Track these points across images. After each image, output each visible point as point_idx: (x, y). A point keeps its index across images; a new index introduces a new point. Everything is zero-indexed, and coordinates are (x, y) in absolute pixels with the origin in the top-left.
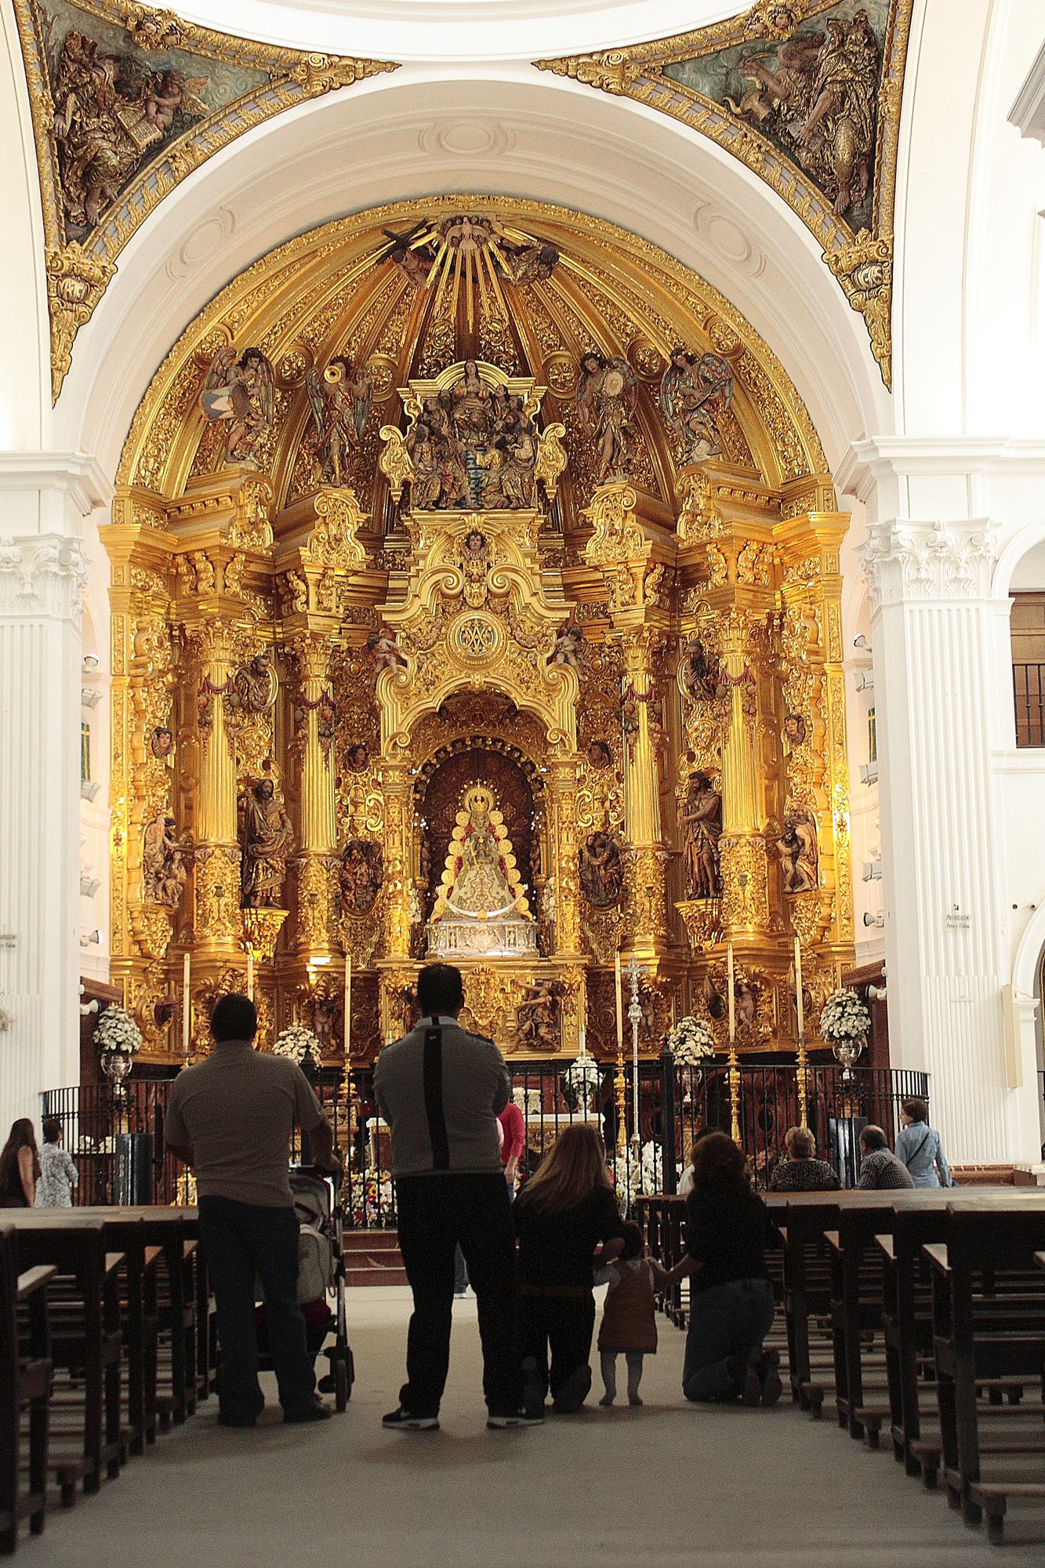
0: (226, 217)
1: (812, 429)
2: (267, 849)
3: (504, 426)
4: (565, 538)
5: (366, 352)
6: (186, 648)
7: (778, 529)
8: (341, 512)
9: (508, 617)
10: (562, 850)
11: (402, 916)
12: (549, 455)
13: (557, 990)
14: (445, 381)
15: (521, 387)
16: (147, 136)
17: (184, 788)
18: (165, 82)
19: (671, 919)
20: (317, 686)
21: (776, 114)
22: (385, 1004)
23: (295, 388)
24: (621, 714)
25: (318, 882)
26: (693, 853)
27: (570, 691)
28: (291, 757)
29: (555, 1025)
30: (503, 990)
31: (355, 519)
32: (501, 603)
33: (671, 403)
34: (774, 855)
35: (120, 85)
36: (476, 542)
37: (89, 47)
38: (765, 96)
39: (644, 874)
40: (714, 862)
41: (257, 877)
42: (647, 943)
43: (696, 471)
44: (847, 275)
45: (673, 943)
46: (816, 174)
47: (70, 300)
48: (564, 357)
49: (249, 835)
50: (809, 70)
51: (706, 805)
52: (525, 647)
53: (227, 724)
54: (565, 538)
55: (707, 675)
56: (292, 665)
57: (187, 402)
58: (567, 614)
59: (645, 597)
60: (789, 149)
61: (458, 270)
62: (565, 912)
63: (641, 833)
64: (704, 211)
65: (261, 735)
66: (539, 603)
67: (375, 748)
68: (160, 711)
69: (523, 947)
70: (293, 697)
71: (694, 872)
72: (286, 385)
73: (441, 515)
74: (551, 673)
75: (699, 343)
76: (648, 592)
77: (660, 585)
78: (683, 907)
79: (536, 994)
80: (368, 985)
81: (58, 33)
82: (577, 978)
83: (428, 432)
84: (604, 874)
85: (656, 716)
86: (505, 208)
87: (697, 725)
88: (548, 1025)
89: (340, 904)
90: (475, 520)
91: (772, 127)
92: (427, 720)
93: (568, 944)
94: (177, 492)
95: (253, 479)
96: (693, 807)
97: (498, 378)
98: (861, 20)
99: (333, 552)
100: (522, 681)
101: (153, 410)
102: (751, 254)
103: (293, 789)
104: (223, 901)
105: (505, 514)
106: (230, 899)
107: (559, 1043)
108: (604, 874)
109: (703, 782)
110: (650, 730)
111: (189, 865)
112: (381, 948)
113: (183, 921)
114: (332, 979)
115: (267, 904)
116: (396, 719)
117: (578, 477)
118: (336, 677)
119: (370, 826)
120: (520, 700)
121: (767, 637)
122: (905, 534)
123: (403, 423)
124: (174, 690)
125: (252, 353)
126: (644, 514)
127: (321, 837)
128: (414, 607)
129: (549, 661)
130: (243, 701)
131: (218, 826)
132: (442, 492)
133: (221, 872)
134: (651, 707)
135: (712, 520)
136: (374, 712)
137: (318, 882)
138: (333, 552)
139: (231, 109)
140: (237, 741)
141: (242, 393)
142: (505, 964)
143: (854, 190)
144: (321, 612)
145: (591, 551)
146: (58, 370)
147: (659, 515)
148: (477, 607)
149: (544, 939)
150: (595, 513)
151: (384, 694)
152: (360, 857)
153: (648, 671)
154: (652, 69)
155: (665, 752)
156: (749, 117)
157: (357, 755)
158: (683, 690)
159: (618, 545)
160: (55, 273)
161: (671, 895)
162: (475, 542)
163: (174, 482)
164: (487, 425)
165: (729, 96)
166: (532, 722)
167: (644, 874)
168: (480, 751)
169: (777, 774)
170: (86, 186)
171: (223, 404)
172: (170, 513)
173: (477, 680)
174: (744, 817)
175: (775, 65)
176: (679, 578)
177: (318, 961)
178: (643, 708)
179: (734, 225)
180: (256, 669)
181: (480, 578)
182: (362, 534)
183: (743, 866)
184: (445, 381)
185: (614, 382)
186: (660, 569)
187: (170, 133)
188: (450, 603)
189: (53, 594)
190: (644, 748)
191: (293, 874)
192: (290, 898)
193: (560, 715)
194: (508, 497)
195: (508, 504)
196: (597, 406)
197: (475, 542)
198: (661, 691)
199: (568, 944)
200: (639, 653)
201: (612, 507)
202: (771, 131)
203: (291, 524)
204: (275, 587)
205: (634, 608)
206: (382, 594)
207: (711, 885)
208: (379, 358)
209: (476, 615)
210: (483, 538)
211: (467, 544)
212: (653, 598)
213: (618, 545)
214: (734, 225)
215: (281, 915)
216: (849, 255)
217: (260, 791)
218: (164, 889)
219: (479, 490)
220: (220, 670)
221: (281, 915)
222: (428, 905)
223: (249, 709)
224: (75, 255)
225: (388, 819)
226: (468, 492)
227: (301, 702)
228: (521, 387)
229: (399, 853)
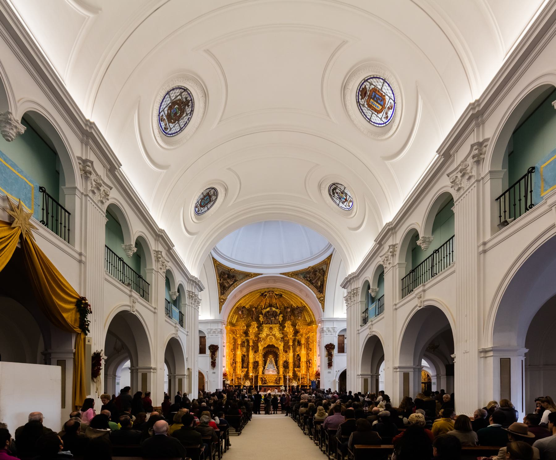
0: (241, 291)
1: (314, 316)
3: (275, 315)
5: (258, 306)
6: (235, 340)
7: (309, 327)
8: (255, 324)
10: (281, 363)
11: (261, 370)
12: (280, 318)
13: (280, 378)
14: (268, 309)
15: (277, 310)
16: (231, 283)
17: (235, 355)
18: (233, 277)
19: (294, 370)
20: (251, 344)
21: (311, 280)
22: (259, 379)
23: (249, 311)
24: (289, 347)
25: (251, 366)
26: (297, 363)
27: (282, 344)
28: (248, 351)
29: (279, 382)
31: (256, 325)
32: (274, 335)
33: (296, 312)
34: (307, 364)
35: (228, 277)
37: (224, 273)
38: (309, 277)
39: (291, 365)
40: (299, 364)
43: (299, 320)
44: (319, 299)
45: (294, 372)
46: (316, 287)
47: (222, 302)
48: (283, 307)
49: (243, 361)
50: (315, 275)
52: (277, 340)
55: (299, 343)
56: (248, 341)
57: (236, 312)
60: (312, 284)
61: (270, 297)
62: (281, 370)
63: (291, 361)
64: (301, 290)
65: (245, 349)
66: (279, 335)
67: (258, 351)
68: (232, 347)
69: (275, 373)
70: (248, 345)
72: (247, 310)
73: (267, 325)
74: (280, 343)
75: (300, 305)
78: (295, 369)
80: (256, 377)
81: (220, 271)
82: (282, 377)
83: (266, 315)
84: (286, 365)
85: (293, 348)
86: (276, 290)
87: (298, 349)
89: (254, 368)
90: (271, 326)
91: (310, 281)
92: (264, 348)
93: (281, 373)
94: (234, 322)
95: (243, 321)
96: (297, 359)
97: (274, 309)
98: (322, 269)
99: (253, 330)
101: (232, 313)
102: (307, 295)
103: (248, 355)
106: (241, 367)
108: (286, 365)
109: (298, 355)
111: (235, 364)
112: (258, 373)
113: (235, 369)
114: (252, 376)
116: (260, 348)
117: (284, 320)
118: (253, 343)
119: (257, 359)
120: (276, 346)
121: (307, 339)
122: (325, 329)
123: (262, 314)
124: (234, 345)
125: (244, 307)
126: (292, 325)
127: (251, 360)
128: (263, 335)
130: (242, 345)
131: (239, 359)
133: (239, 365)
135: (301, 327)
136: (258, 347)
137: (251, 366)
138: (253, 330)
139: (241, 279)
140: (241, 349)
141: (242, 312)
142: (273, 375)
143: (321, 289)
144: (252, 337)
145: (285, 329)
146: (220, 310)
147: (294, 325)
148: (271, 335)
149: (278, 373)
150: (286, 325)
151: (259, 344)
152: (256, 364)
154: (295, 274)
155: (294, 351)
156: (307, 280)
157: (256, 351)
159: (289, 329)
160: (220, 299)
161: (294, 368)
162: (271, 328)
163: (234, 321)
164: (273, 315)
165: (305, 277)
166: (278, 348)
167: (291, 365)
168: (271, 351)
169: (308, 354)
170: (223, 289)
171: (240, 313)
172: (233, 325)
173: (271, 344)
174: (303, 359)
175: (311, 274)
176: (296, 332)
177: (251, 374)
179: (305, 294)
180: (244, 342)
182: (257, 327)
183: (303, 365)
184: (268, 309)
185: (289, 310)
187: (234, 283)
188: (268, 335)
189: (219, 335)
190: (291, 351)
191: (248, 365)
192: (247, 367)
193: (281, 348)
195: (275, 324)
196: (287, 312)
197: (271, 328)
198: (294, 344)
199: (281, 373)
201: (288, 324)
202: (310, 282)
203: (248, 326)
204: (246, 333)
205: (290, 336)
206: (259, 334)
207: (299, 367)
208: (259, 307)
213: (289, 329)
214: (305, 294)
215: (246, 369)
216: (319, 296)
217: (244, 356)
220: (239, 342)
221: (246, 369)
222: (264, 368)
223: (243, 347)
224: (222, 297)
225: (260, 360)
227: (249, 346)
228: (277, 310)
229: (261, 363)
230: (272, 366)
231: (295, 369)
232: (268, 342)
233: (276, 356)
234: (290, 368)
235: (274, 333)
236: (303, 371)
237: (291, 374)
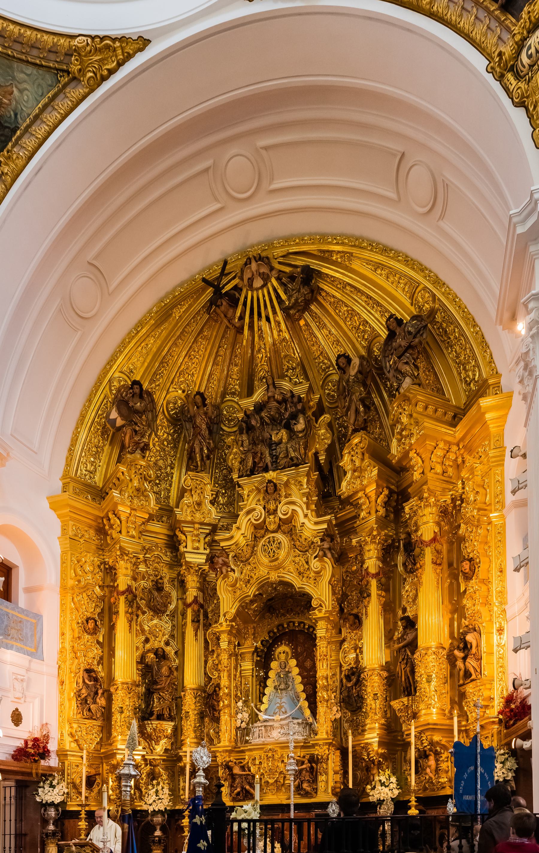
2: (159, 687)
4: (327, 479)
9: (291, 535)
13: (313, 760)
25: (190, 705)
30: (283, 761)
32: (287, 526)
36: (271, 489)
39: (374, 686)
41: (153, 703)
42: (373, 728)
51: (409, 637)
53: (127, 612)
54: (327, 479)
58: (325, 526)
59: (377, 511)
62: (328, 713)
68: (90, 609)
71: (402, 681)
74: (315, 564)
76: (379, 508)
77: (385, 503)
79: (303, 763)
88: (309, 781)
90: (271, 475)
100: (300, 573)
103: (180, 653)
104: (123, 716)
105: (291, 471)
107: (316, 793)
110: (378, 595)
115: (160, 717)
116: (228, 604)
129: (315, 557)
132: (254, 463)
134: (379, 581)
137: (190, 705)
153: (378, 558)
158: (400, 568)
159: (361, 481)
162: (272, 491)
167: (374, 686)
168: (281, 618)
178: (374, 583)
181: (275, 511)
186: (386, 492)
188: (260, 529)
191: (178, 701)
194: (292, 459)
197: (272, 491)
200: (372, 547)
207: (410, 689)
209: (273, 535)
210: (275, 485)
211: (267, 491)
212: (382, 511)
217: (161, 655)
218: (89, 710)
219: (275, 459)
226: (268, 459)
230: (285, 699)
231: (396, 704)
232: (263, 569)
233: (304, 643)
234: (369, 700)
235: (283, 510)
236: (432, 704)
237: (373, 737)
